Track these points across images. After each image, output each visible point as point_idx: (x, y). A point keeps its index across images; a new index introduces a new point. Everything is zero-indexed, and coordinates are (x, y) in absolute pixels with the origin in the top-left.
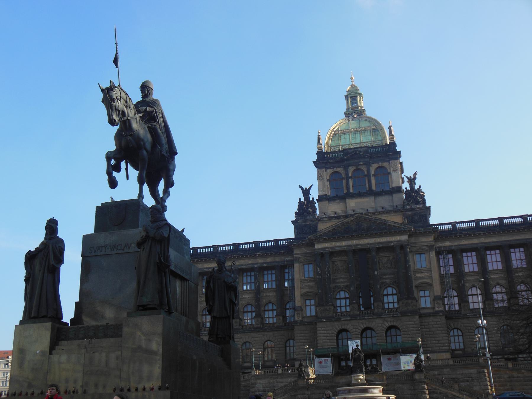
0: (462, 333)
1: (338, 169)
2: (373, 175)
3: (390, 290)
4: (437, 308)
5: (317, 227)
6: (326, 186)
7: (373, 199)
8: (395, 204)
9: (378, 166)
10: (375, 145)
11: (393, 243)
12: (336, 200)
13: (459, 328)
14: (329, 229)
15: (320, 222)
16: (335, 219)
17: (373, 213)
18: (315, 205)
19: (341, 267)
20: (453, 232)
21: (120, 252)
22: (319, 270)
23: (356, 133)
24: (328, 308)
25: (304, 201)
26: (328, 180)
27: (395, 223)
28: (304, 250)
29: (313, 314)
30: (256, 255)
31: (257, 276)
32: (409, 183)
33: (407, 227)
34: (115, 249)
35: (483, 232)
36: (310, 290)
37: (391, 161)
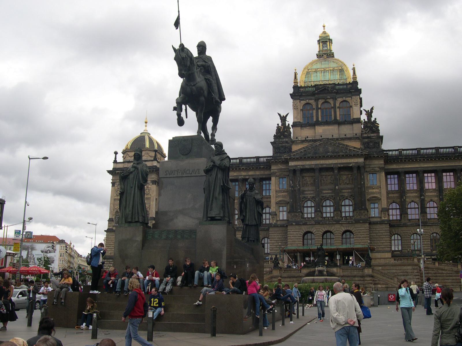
0: (401, 238)
1: (309, 101)
2: (339, 107)
3: (347, 202)
4: (384, 217)
5: (291, 149)
6: (300, 115)
7: (337, 127)
8: (355, 132)
9: (343, 100)
10: (340, 83)
11: (351, 164)
12: (307, 126)
13: (399, 234)
14: (301, 151)
15: (294, 144)
16: (305, 142)
17: (337, 139)
18: (290, 130)
19: (309, 181)
20: (400, 157)
21: (189, 175)
22: (291, 183)
23: (326, 72)
24: (297, 214)
25: (281, 126)
26: (302, 110)
27: (355, 148)
28: (281, 166)
29: (285, 218)
30: (240, 168)
31: (241, 185)
32: (367, 115)
33: (364, 151)
34: (185, 173)
36: (283, 199)
37: (353, 97)
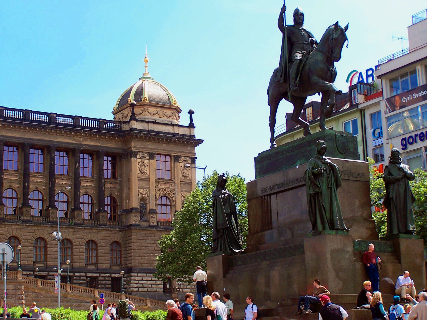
21: (355, 179)
35: (8, 124)
